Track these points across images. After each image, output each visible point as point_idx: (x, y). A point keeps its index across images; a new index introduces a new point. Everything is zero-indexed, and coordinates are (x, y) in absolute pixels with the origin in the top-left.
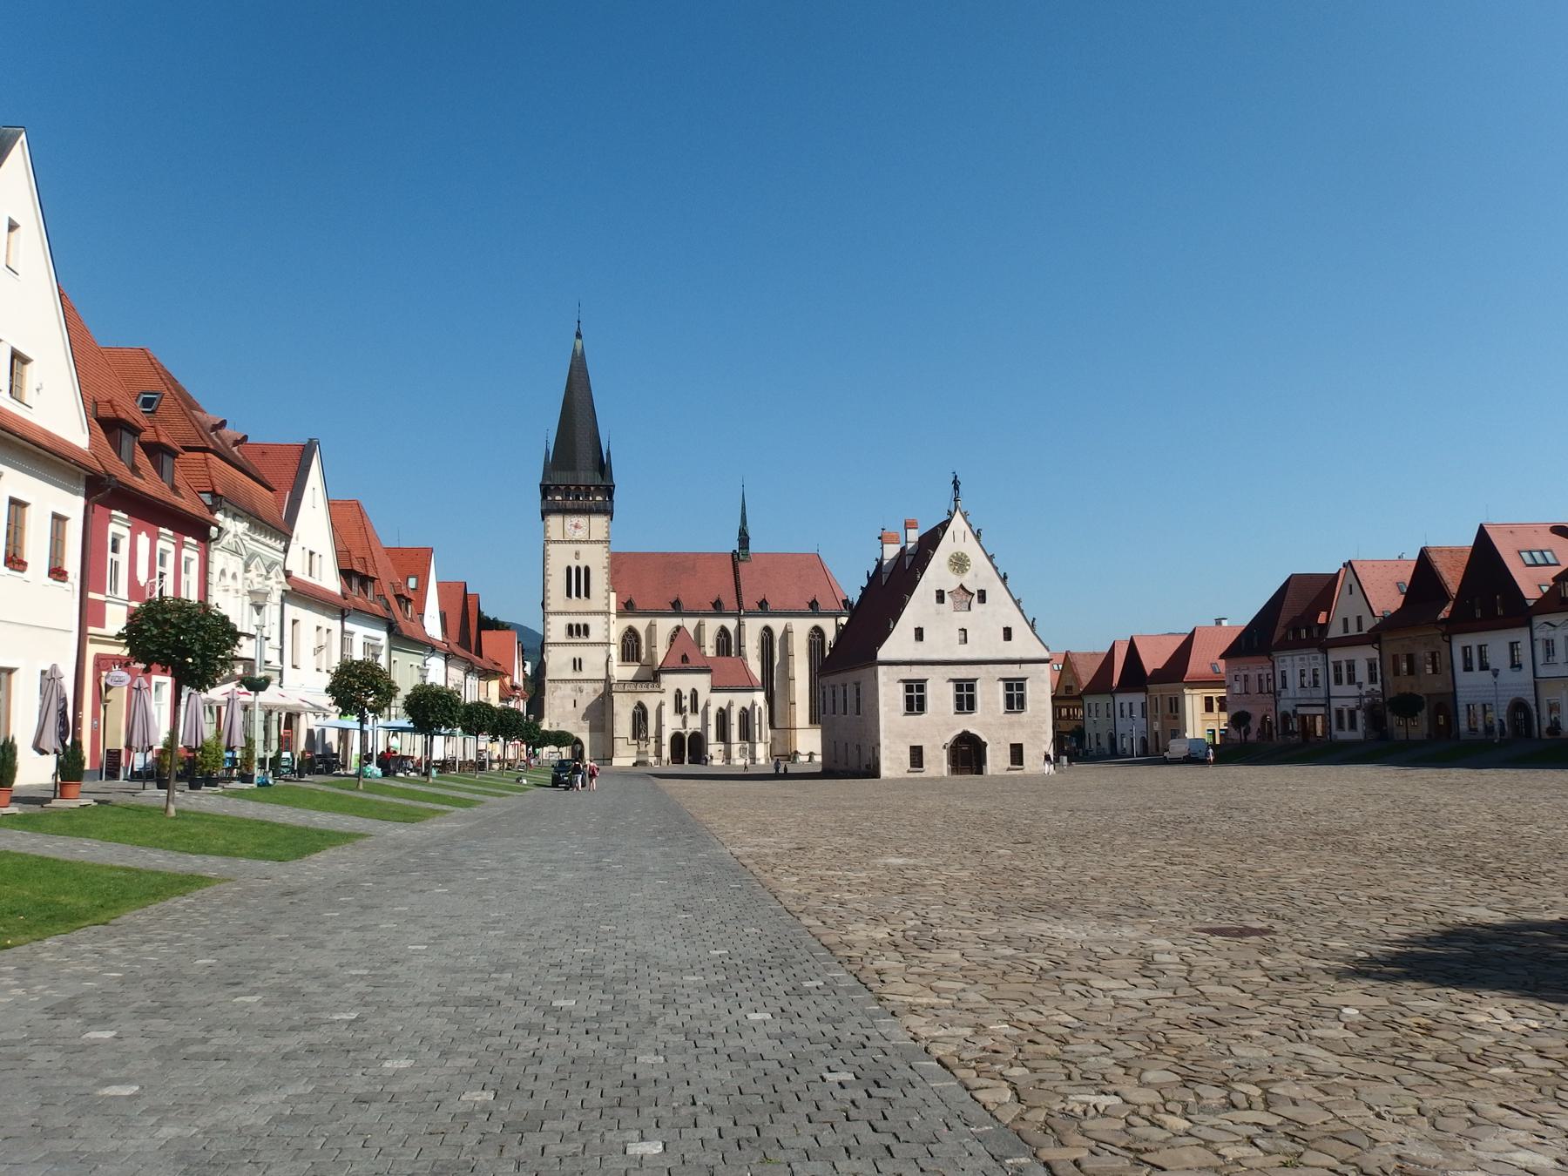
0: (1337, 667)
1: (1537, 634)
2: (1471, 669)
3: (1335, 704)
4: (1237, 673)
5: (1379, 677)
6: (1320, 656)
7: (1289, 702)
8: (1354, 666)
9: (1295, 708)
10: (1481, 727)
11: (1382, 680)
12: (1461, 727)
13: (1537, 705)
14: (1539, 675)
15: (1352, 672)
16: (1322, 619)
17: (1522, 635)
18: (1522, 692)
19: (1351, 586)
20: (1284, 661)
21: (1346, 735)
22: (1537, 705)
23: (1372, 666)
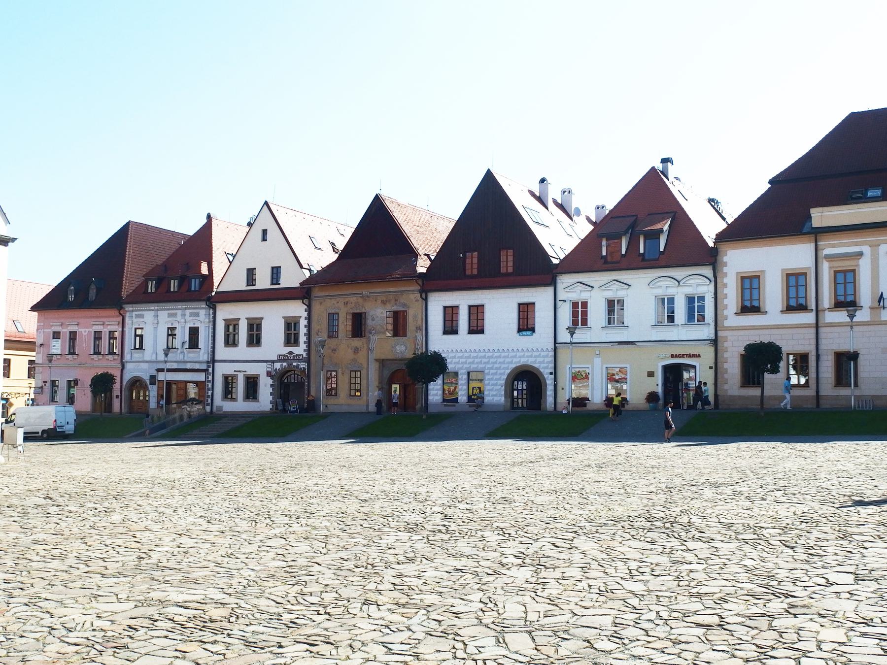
0: (231, 326)
1: (561, 295)
2: (455, 332)
3: (221, 370)
4: (57, 329)
5: (303, 338)
6: (202, 313)
7: (145, 366)
8: (259, 327)
9: (154, 373)
10: (463, 398)
11: (309, 342)
12: (430, 398)
13: (555, 373)
14: (558, 342)
15: (293, 332)
16: (204, 270)
17: (541, 297)
18: (532, 360)
19: (265, 232)
20: (142, 316)
21: (240, 405)
22: (555, 373)
23: (291, 326)
